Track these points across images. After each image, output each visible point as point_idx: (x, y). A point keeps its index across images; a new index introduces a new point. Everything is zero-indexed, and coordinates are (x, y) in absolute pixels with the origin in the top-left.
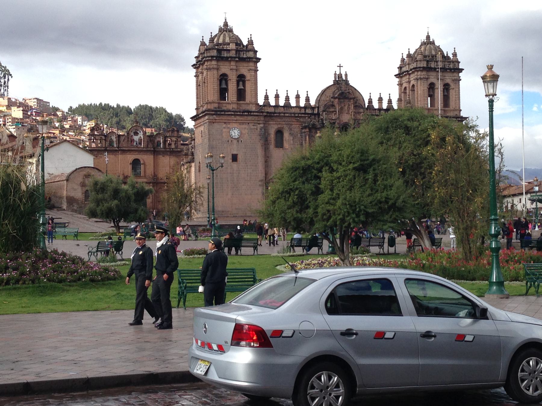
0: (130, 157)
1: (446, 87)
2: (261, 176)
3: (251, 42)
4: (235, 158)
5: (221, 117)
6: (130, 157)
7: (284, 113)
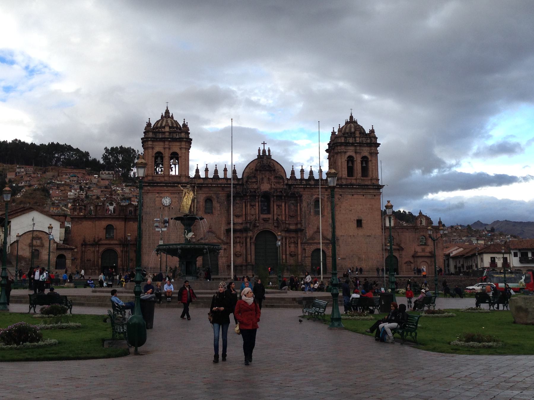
0: (104, 223)
1: (365, 160)
5: (155, 188)
6: (104, 223)
7: (211, 184)
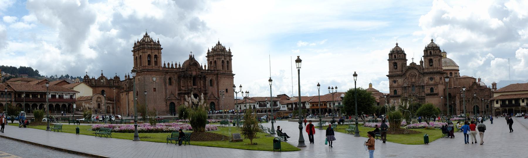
1: (227, 61)
2: (164, 97)
3: (158, 42)
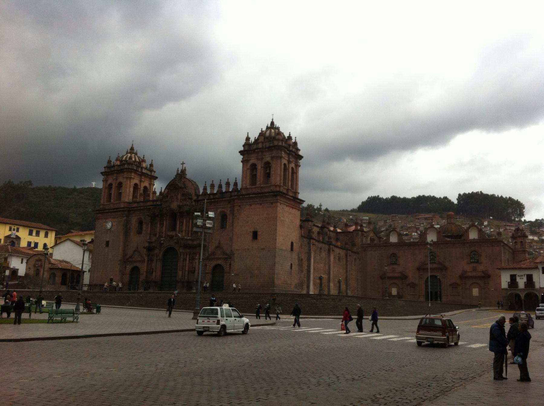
4: (107, 244)
